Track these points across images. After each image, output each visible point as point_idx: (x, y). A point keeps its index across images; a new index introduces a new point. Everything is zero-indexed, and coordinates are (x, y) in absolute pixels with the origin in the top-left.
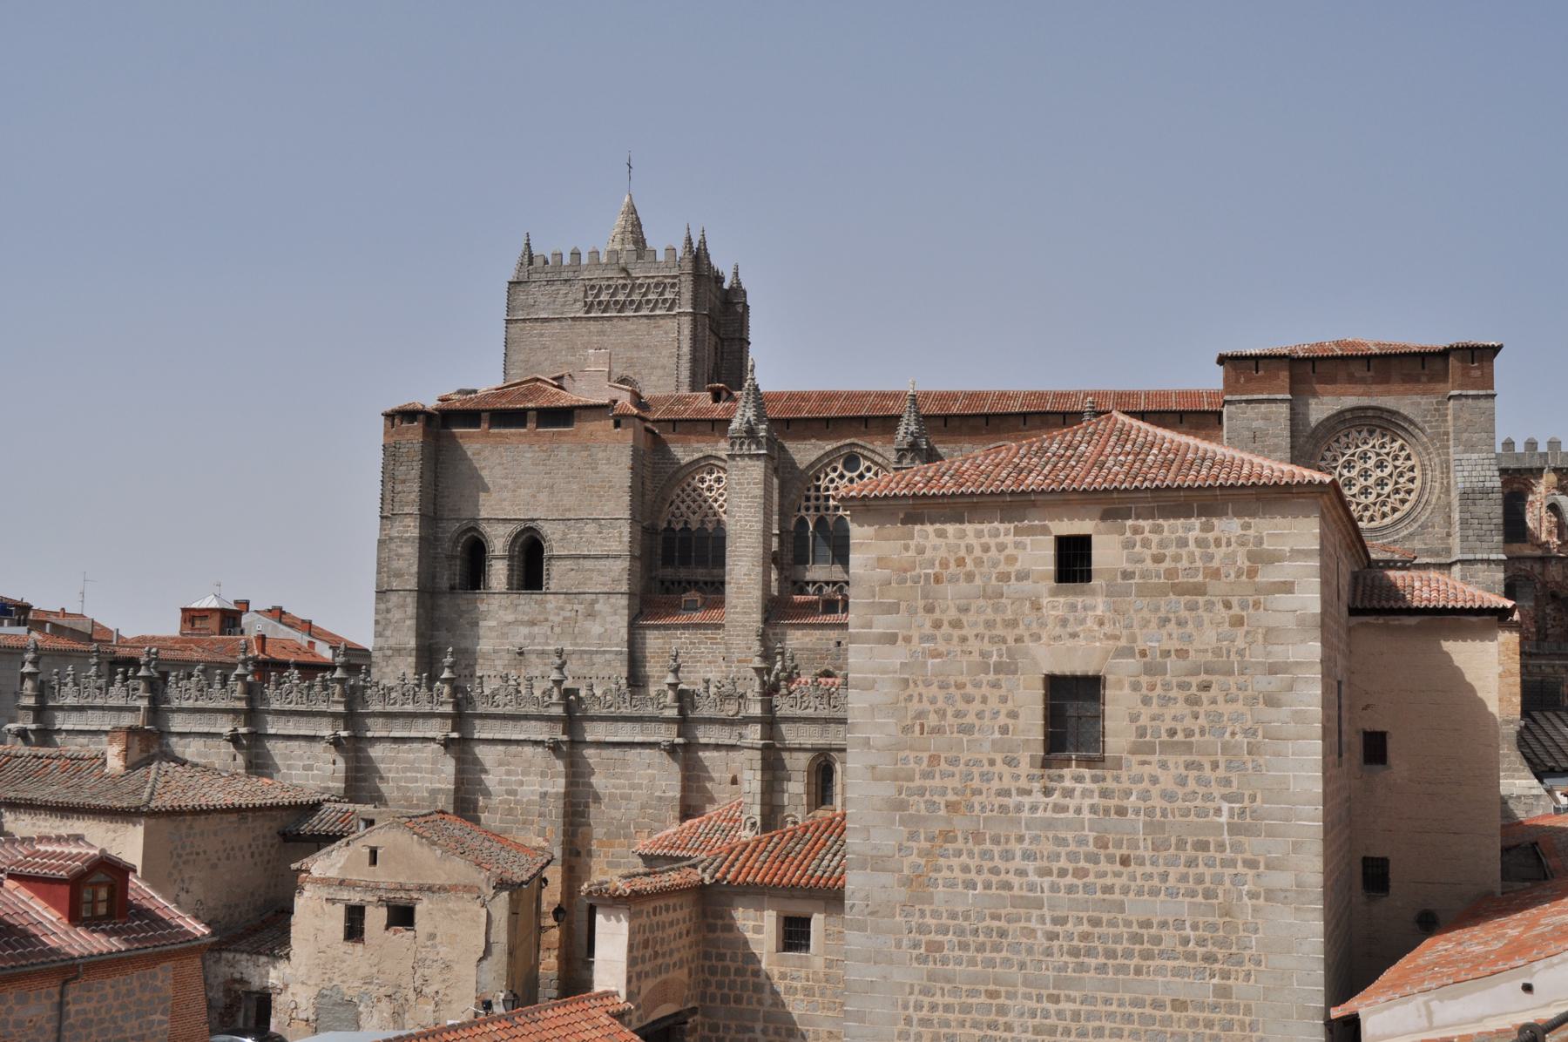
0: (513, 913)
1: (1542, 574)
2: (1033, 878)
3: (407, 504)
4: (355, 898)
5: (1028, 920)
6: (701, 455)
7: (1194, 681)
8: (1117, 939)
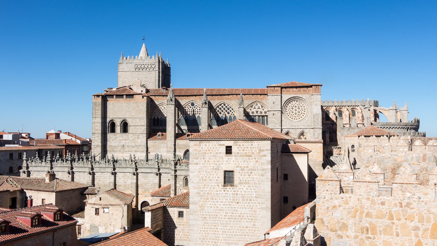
0: (128, 209)
1: (333, 127)
2: (222, 206)
3: (98, 115)
4: (97, 207)
5: (221, 213)
7: (250, 172)
8: (236, 216)
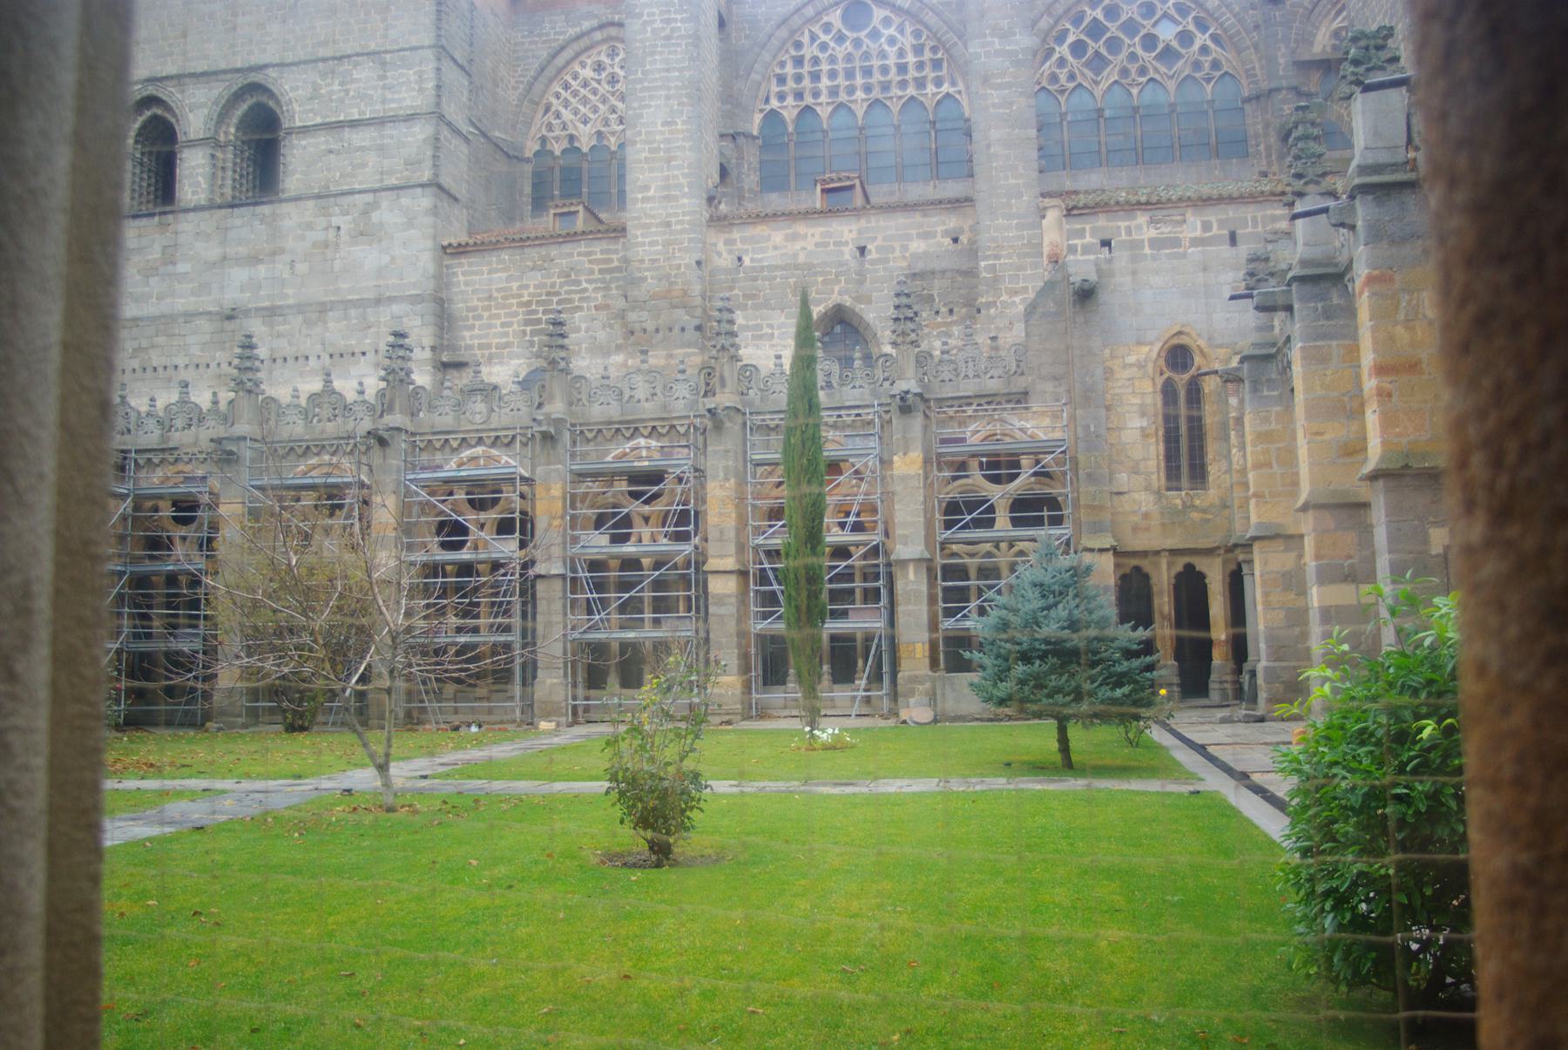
6: (595, 23)
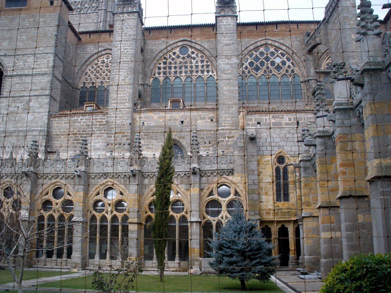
6: (103, 49)
